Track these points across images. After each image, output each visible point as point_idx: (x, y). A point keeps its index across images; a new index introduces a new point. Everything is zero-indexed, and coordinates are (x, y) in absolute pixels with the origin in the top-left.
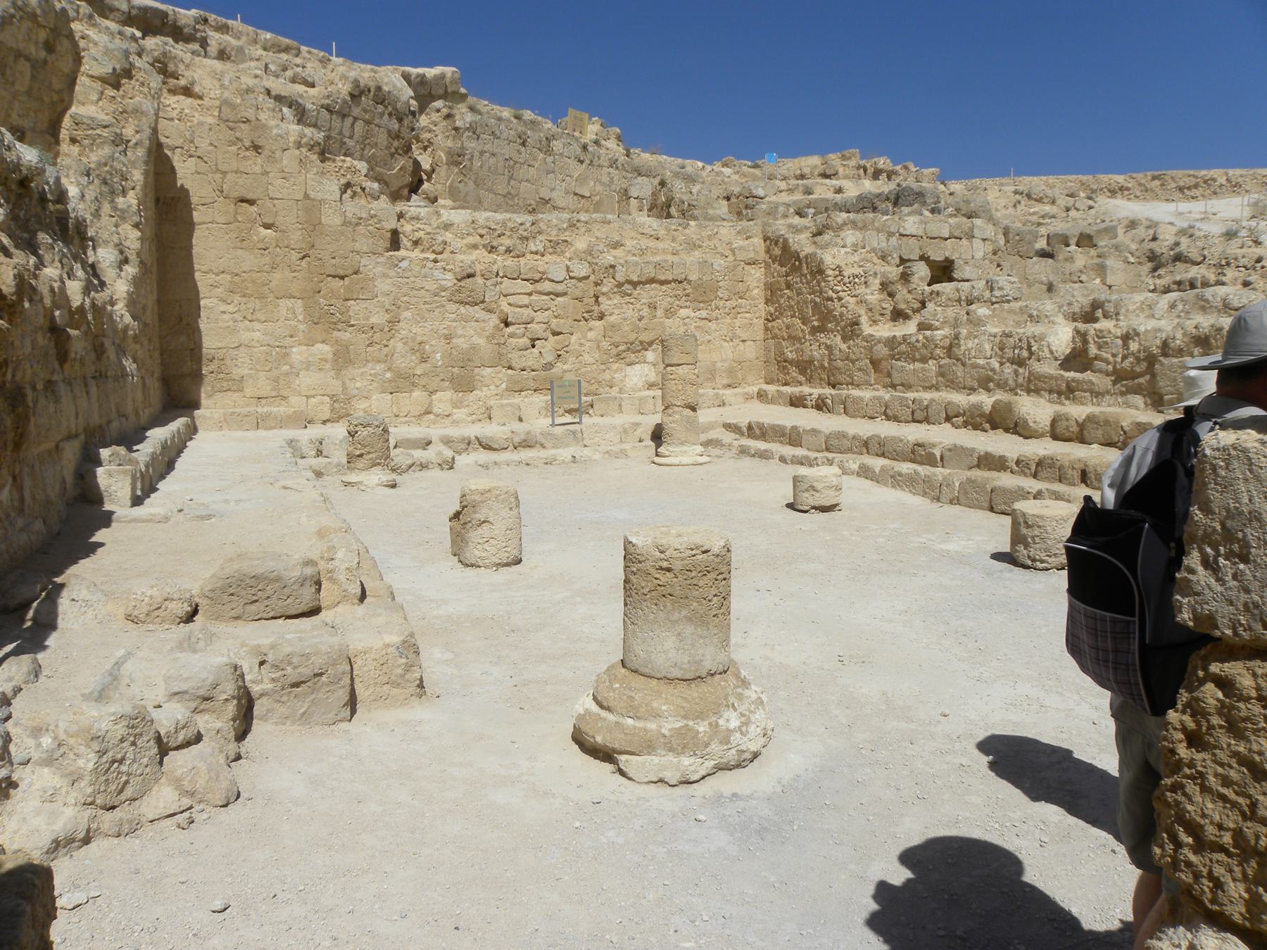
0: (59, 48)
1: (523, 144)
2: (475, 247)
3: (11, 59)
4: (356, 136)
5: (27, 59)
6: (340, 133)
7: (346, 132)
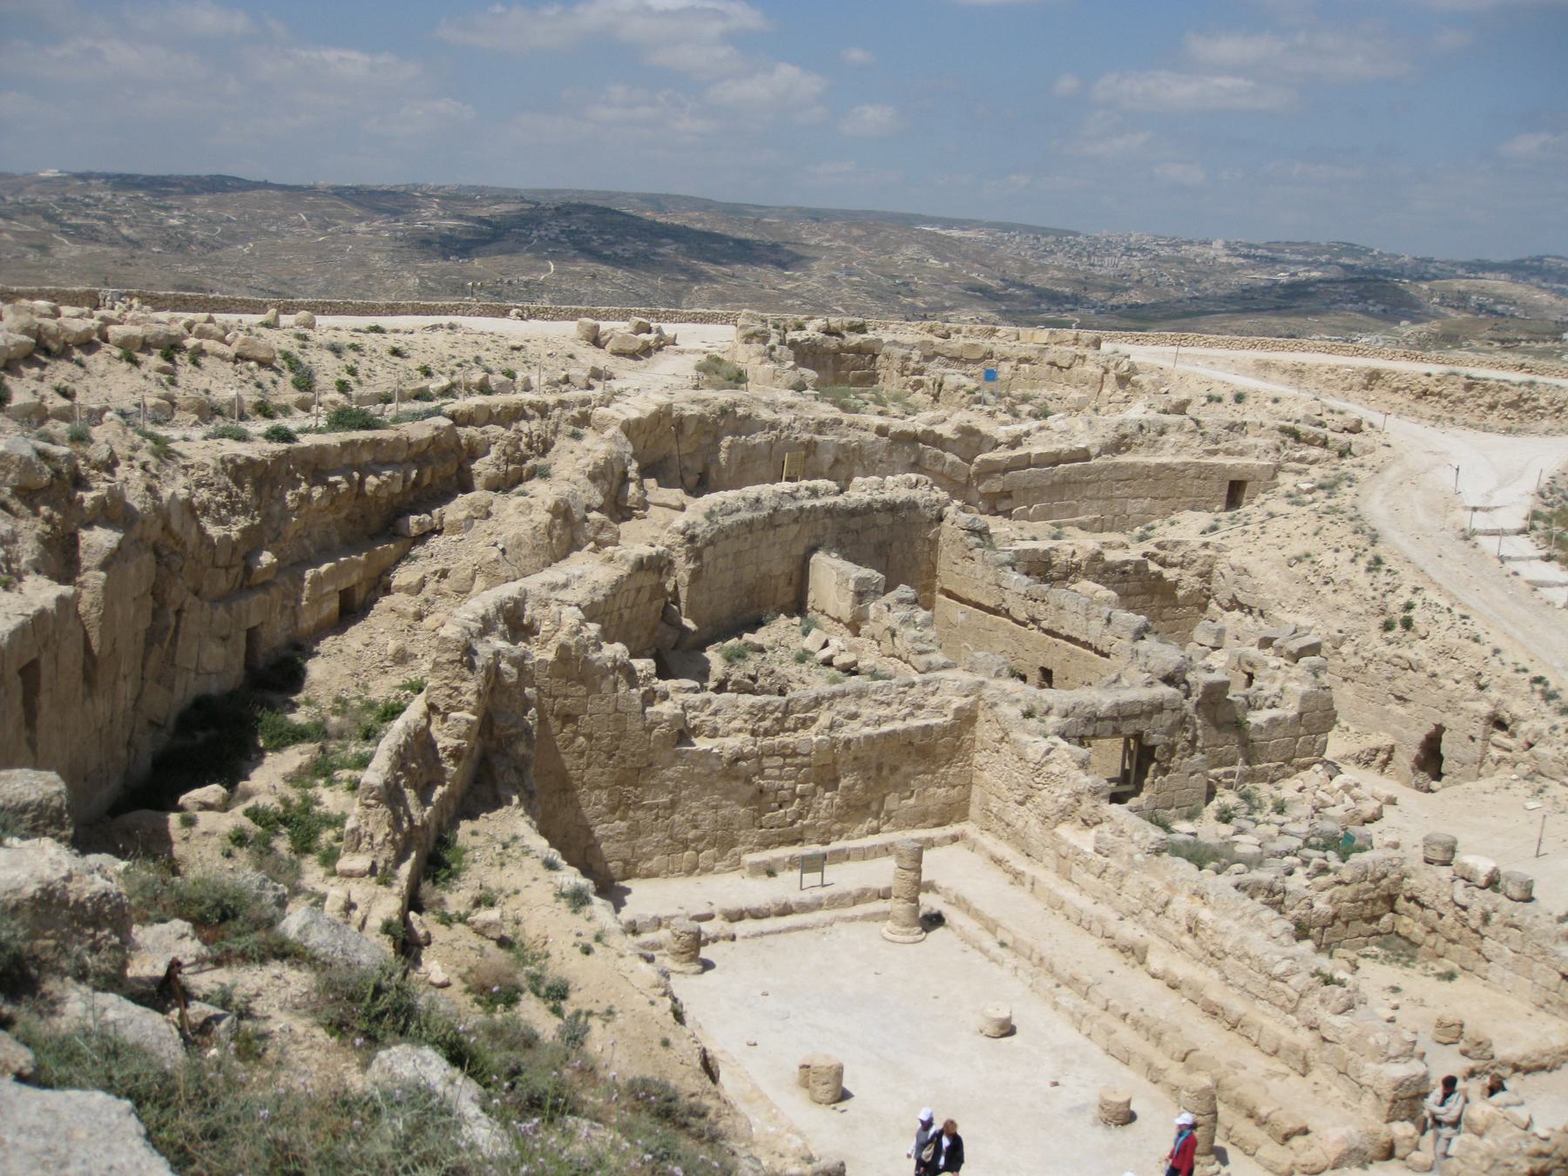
2: (740, 730)
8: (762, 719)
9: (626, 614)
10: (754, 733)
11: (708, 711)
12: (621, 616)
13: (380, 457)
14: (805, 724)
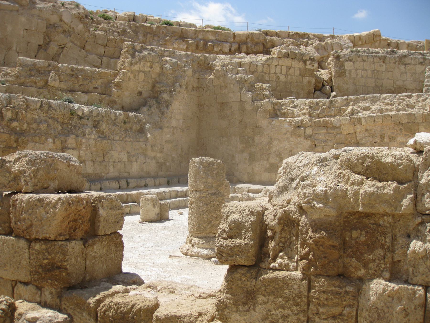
0: (154, 66)
1: (384, 62)
2: (304, 114)
3: (137, 74)
4: (283, 73)
5: (143, 72)
6: (275, 73)
7: (278, 71)
8: (314, 109)
9: (282, 78)
10: (310, 116)
11: (291, 106)
12: (278, 78)
13: (219, 38)
14: (340, 112)
